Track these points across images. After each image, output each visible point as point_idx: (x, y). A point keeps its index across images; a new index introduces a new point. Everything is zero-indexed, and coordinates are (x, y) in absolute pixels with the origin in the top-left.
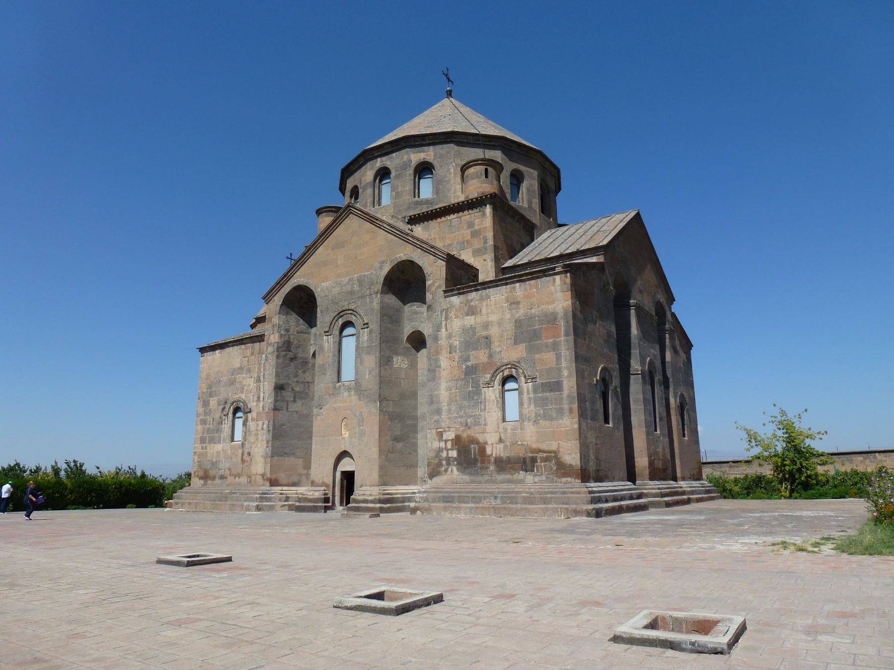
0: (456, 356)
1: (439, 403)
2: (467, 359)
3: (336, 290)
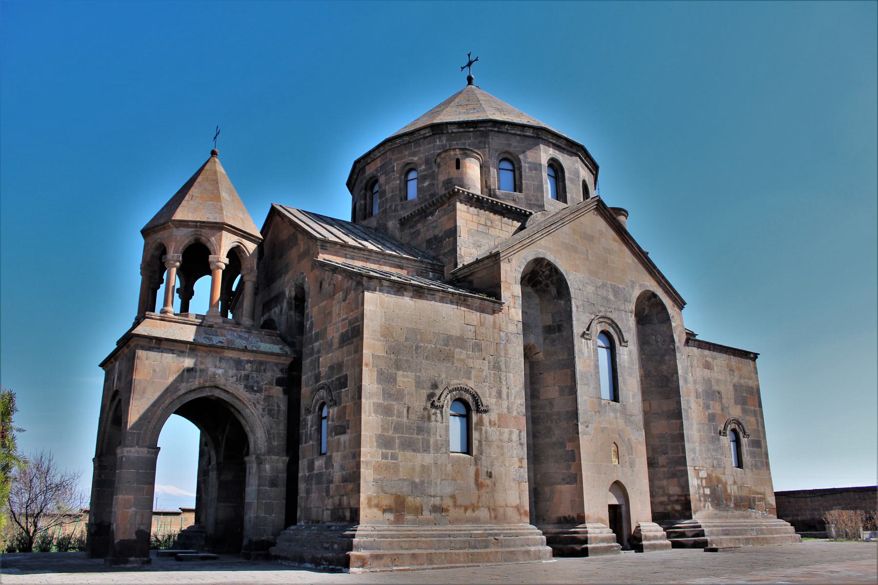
0: (701, 401)
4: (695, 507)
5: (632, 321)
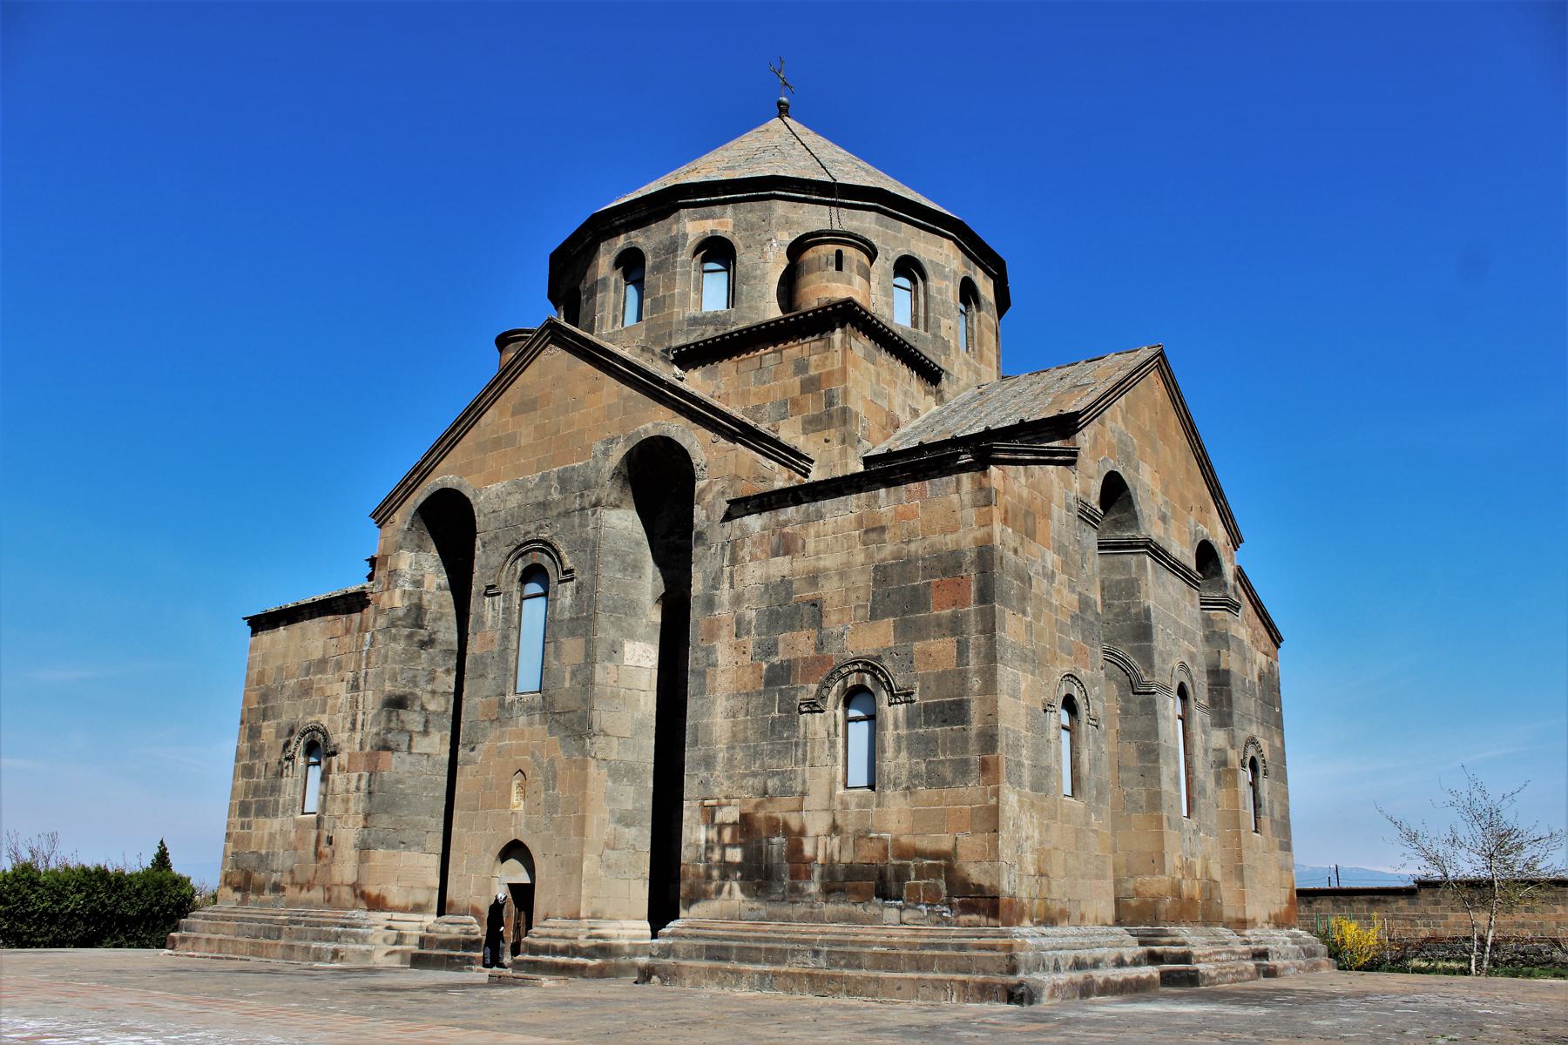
0: (750, 641)
1: (709, 744)
2: (771, 650)
3: (514, 501)
4: (692, 889)
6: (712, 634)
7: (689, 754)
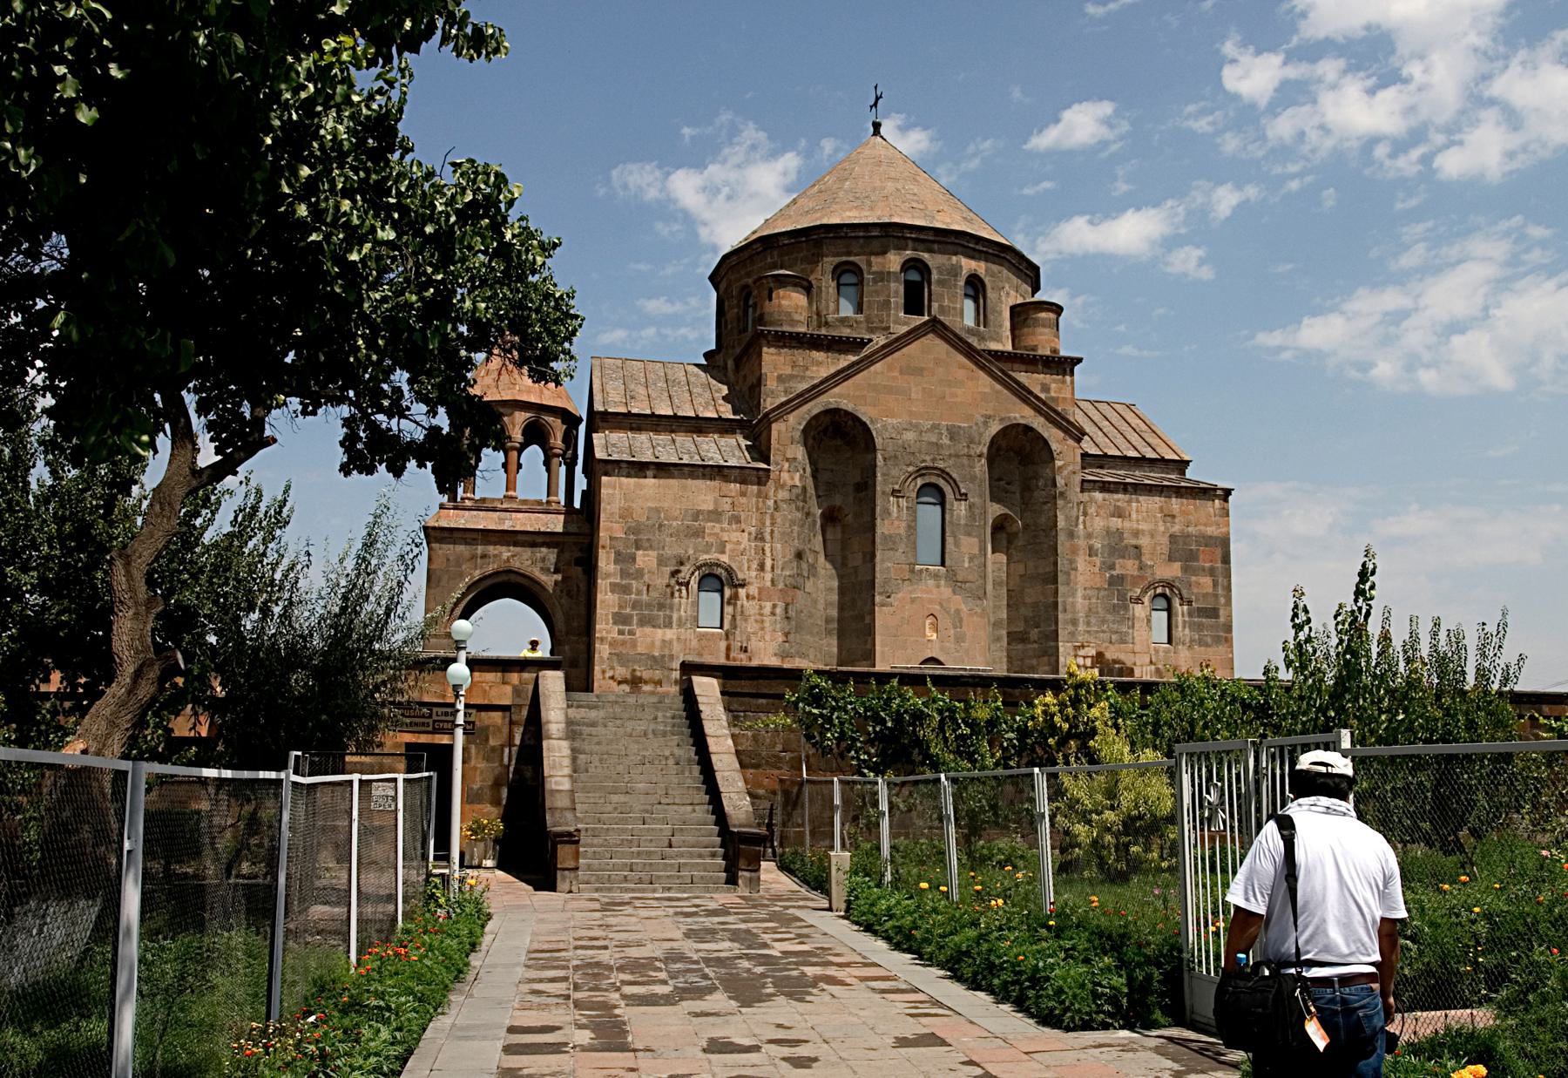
0: (1098, 560)
1: (1074, 612)
2: (1112, 567)
5: (981, 467)
6: (1074, 551)
7: (1061, 616)
